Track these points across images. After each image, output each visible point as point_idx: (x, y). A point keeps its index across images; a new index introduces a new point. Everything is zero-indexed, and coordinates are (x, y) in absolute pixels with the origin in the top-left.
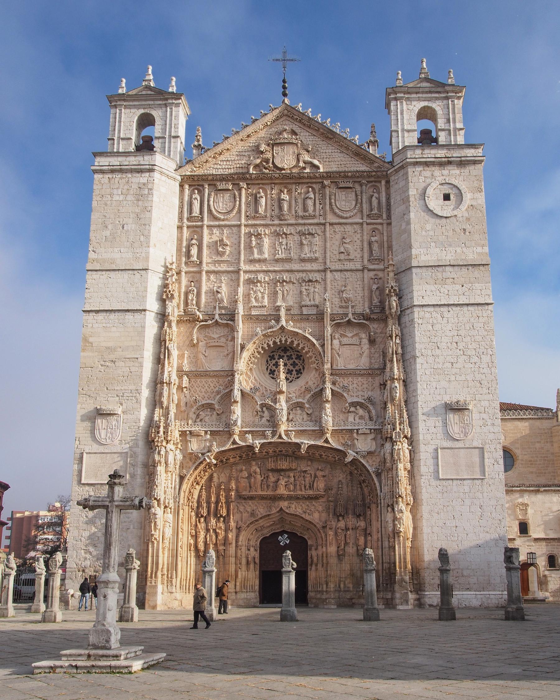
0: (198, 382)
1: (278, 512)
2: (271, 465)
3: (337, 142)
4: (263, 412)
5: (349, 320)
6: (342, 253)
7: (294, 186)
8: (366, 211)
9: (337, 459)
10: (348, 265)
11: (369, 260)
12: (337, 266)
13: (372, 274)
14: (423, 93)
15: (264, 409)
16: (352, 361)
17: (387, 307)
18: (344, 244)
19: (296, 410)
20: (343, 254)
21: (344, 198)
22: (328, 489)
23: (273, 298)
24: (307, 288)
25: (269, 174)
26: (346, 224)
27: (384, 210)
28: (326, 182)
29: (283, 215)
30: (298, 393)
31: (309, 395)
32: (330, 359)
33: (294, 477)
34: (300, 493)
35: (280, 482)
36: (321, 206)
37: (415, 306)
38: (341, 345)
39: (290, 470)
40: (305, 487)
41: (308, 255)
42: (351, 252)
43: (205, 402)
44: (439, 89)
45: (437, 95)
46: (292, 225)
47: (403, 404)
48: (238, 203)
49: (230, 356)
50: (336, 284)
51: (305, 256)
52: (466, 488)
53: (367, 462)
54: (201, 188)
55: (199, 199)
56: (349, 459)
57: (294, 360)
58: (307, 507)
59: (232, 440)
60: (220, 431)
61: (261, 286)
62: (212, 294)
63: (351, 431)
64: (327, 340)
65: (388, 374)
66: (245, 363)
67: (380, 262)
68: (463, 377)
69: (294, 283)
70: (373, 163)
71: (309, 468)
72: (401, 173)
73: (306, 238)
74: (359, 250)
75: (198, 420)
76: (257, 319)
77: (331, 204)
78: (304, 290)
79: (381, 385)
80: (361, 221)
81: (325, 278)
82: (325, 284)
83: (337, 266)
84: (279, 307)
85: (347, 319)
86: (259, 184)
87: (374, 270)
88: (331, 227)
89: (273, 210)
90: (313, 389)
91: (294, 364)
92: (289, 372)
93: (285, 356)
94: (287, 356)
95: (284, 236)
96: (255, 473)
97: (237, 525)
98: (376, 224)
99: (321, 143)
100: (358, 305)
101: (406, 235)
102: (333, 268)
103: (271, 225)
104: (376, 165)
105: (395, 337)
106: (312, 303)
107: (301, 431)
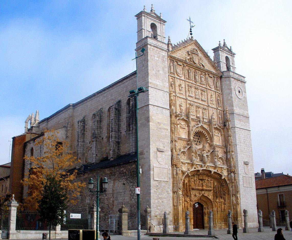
2: (201, 178)
3: (208, 59)
6: (212, 101)
14: (226, 51)
22: (214, 188)
34: (208, 188)
37: (236, 127)
44: (230, 52)
45: (229, 53)
46: (198, 86)
52: (249, 190)
56: (223, 178)
57: (198, 137)
68: (246, 154)
70: (217, 71)
72: (227, 79)
76: (193, 120)
86: (189, 66)
91: (198, 139)
99: (203, 57)
101: (231, 101)
104: (218, 72)
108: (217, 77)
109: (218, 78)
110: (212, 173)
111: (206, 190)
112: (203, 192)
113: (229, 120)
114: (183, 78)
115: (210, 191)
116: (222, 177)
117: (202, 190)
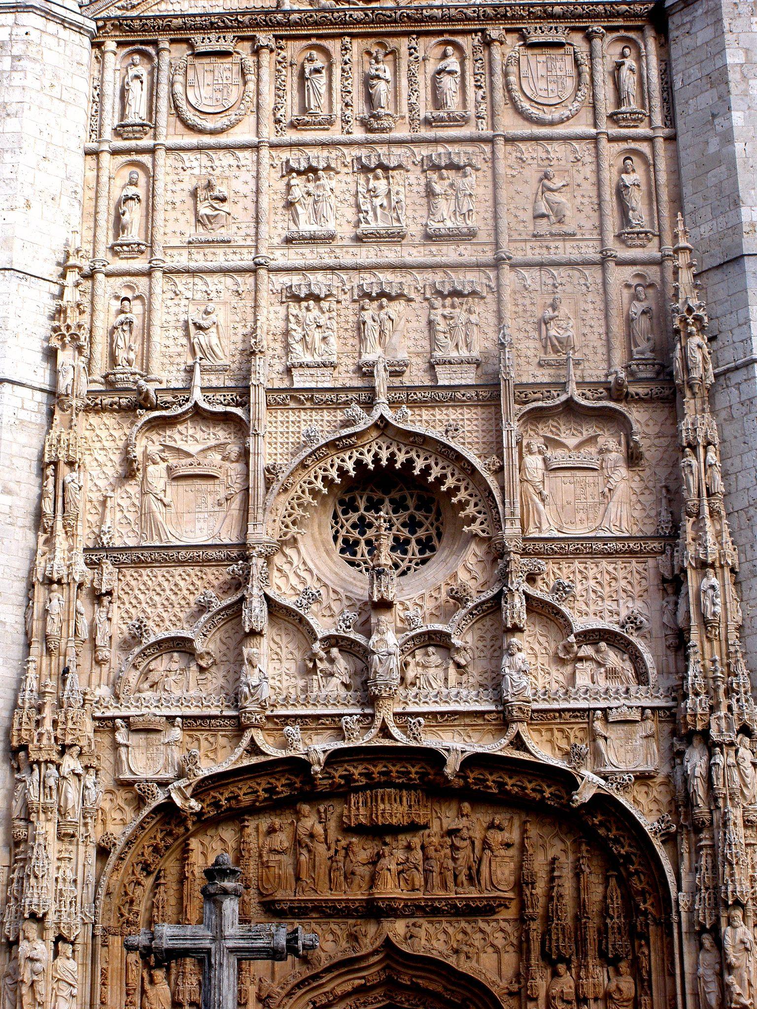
0: (145, 578)
1: (375, 952)
4: (332, 661)
5: (570, 401)
6: (543, 216)
7: (403, 44)
8: (606, 106)
9: (547, 795)
10: (561, 251)
11: (618, 236)
12: (529, 252)
13: (628, 273)
15: (335, 651)
16: (581, 515)
17: (678, 364)
18: (548, 194)
19: (427, 654)
20: (545, 220)
21: (542, 71)
22: (522, 883)
23: (351, 341)
24: (447, 312)
25: (338, 11)
26: (550, 139)
27: (657, 102)
28: (494, 32)
29: (377, 117)
30: (429, 605)
31: (464, 611)
32: (518, 511)
33: (423, 848)
34: (442, 894)
35: (384, 862)
36: (481, 92)
38: (550, 469)
39: (413, 828)
40: (456, 877)
41: (449, 224)
42: (568, 213)
43: (167, 635)
47: (733, 636)
48: (251, 86)
49: (236, 504)
50: (527, 302)
51: (441, 225)
53: (635, 801)
54: (151, 50)
55: (145, 78)
56: (584, 795)
57: (412, 510)
58: (460, 936)
59: (245, 742)
60: (211, 717)
61: (321, 309)
62: (180, 333)
63: (587, 712)
64: (510, 456)
65: (691, 551)
66: (278, 523)
67: (649, 240)
69: (410, 300)
71: (462, 823)
73: (442, 178)
74: (588, 210)
75: (146, 686)
76: (311, 399)
77: (507, 86)
78: (439, 319)
79: (664, 580)
80: (593, 131)
81: (499, 286)
82: (499, 301)
83: (529, 252)
84: (373, 365)
85: (563, 398)
87: (633, 263)
88: (509, 148)
89: (347, 105)
90: (474, 593)
91: (412, 525)
92: (400, 545)
93: (387, 502)
94: (392, 501)
95: (379, 171)
96: (312, 836)
97: (260, 989)
98: (635, 139)
100: (590, 357)
102: (518, 257)
103: (344, 144)
105: (705, 447)
106: (464, 353)
107: (443, 714)
108: (620, 22)
109: (639, 29)
110: (452, 765)
111: (419, 908)
112: (398, 928)
113: (684, 321)
114: (244, 134)
115: (485, 910)
116: (577, 786)
117: (375, 911)
